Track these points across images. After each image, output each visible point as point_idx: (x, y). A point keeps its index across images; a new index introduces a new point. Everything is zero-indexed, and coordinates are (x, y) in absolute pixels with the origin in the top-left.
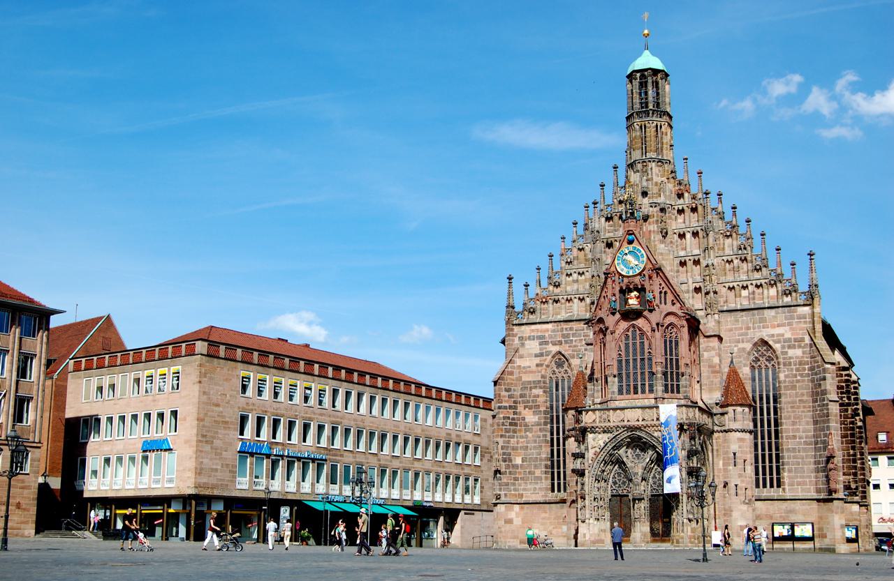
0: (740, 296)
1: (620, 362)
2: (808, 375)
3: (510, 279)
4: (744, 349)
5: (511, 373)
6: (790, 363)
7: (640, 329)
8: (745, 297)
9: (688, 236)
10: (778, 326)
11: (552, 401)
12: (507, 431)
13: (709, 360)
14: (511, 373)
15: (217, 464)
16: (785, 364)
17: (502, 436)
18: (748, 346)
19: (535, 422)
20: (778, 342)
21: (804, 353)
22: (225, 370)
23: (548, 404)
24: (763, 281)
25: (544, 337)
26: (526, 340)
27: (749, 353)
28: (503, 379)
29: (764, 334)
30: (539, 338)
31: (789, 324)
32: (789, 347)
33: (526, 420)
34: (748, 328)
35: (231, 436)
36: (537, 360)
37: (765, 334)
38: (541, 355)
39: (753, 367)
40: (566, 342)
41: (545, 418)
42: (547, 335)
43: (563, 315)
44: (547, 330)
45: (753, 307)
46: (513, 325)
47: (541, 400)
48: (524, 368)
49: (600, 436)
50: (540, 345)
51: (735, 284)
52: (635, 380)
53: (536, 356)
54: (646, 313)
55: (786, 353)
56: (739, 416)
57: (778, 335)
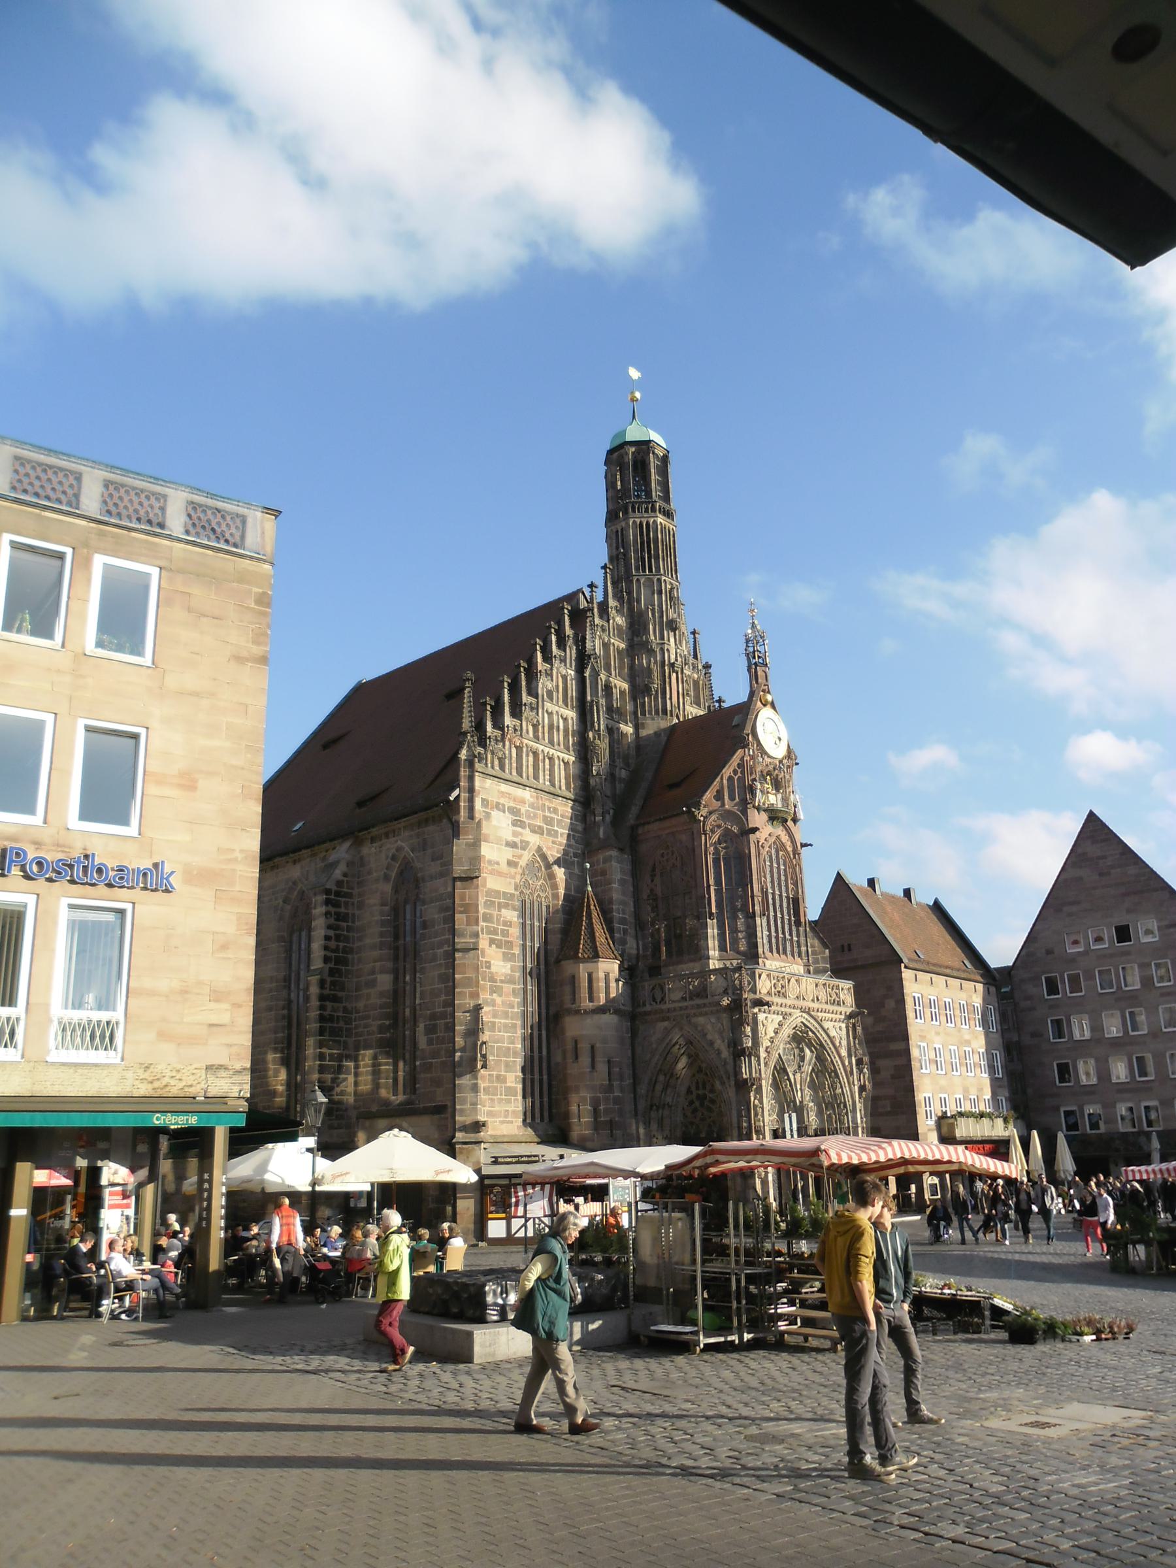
19: (506, 975)
26: (492, 808)
33: (494, 969)
36: (508, 853)
38: (513, 845)
40: (549, 833)
42: (523, 810)
44: (523, 802)
50: (514, 823)
53: (508, 844)
54: (790, 823)
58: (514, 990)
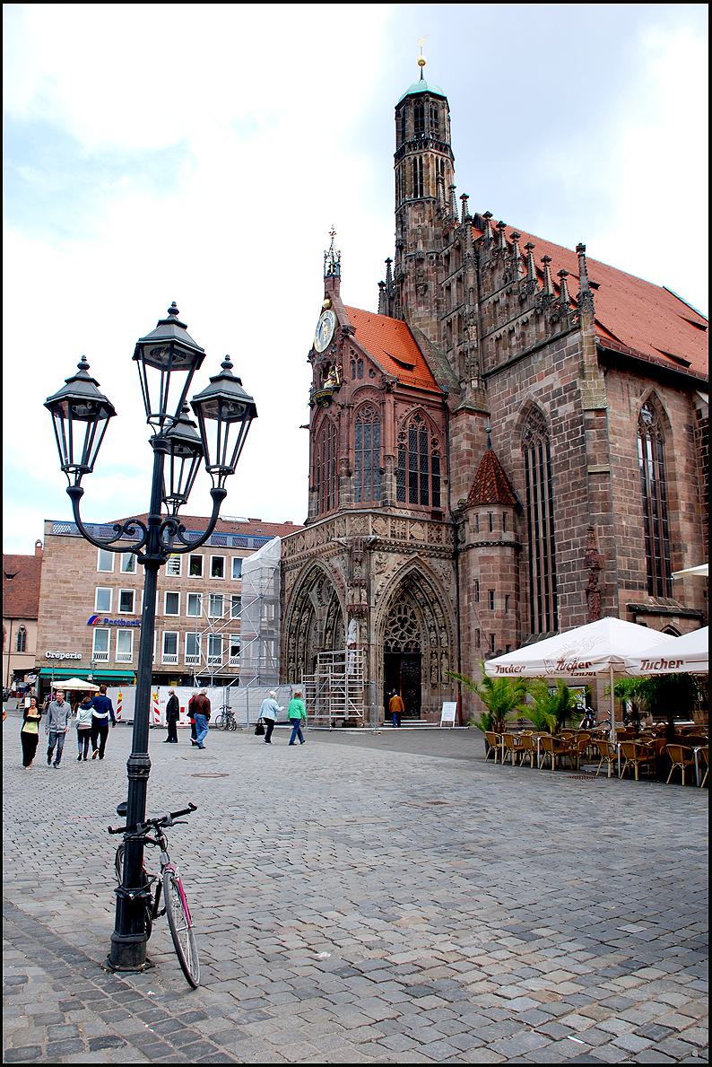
15: (65, 638)
18: (515, 416)
20: (544, 400)
22: (77, 548)
27: (518, 427)
34: (515, 390)
35: (85, 611)
39: (525, 448)
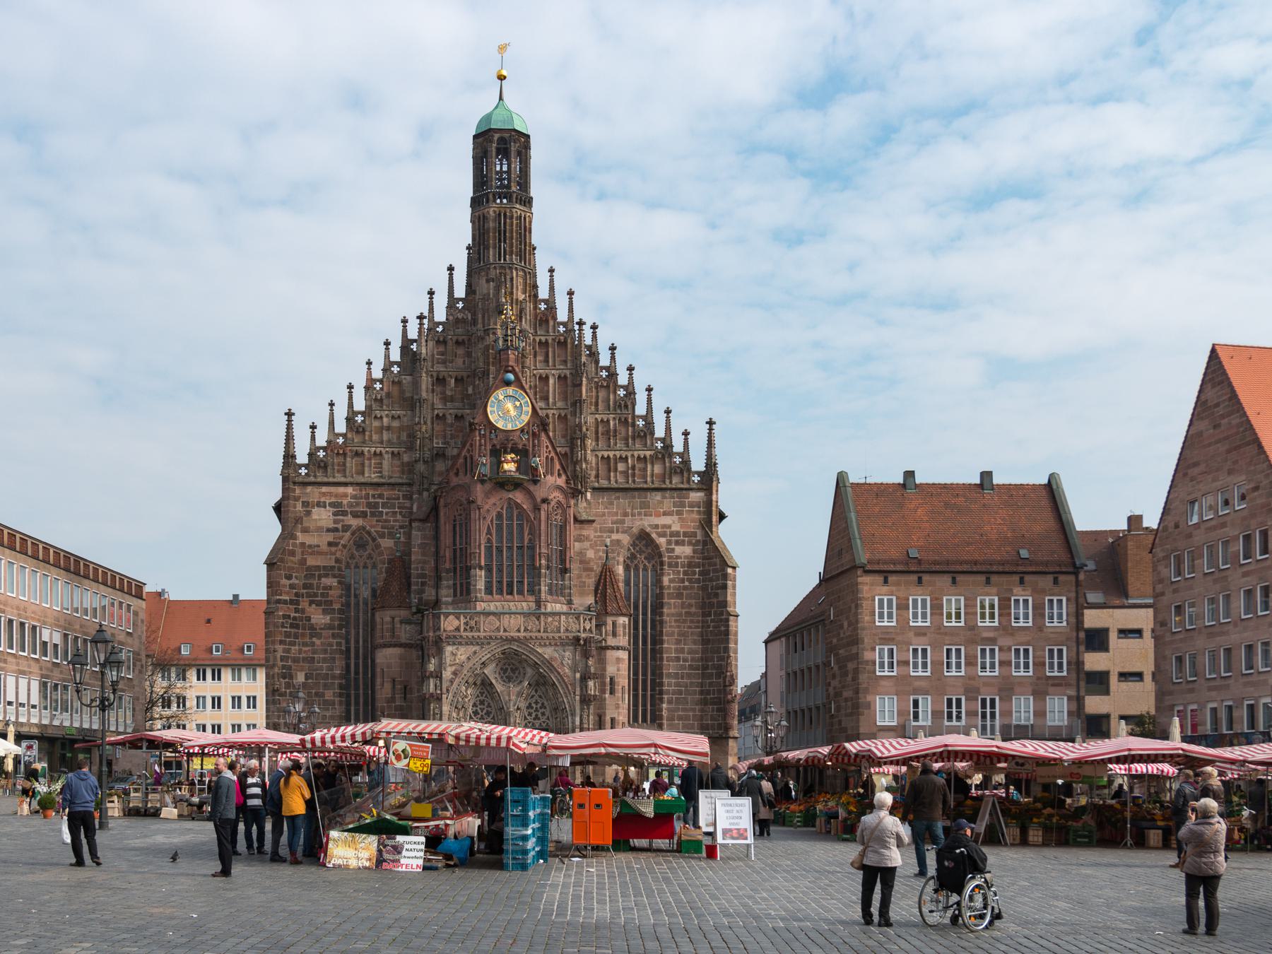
0: (616, 470)
1: (489, 549)
2: (698, 581)
3: (289, 414)
4: (618, 541)
5: (293, 553)
6: (676, 565)
7: (518, 506)
8: (621, 472)
9: (551, 381)
10: (665, 514)
11: (349, 596)
12: (287, 635)
13: (581, 553)
14: (293, 553)
16: (670, 565)
17: (281, 642)
18: (626, 539)
20: (660, 535)
21: (694, 551)
23: (343, 600)
24: (648, 453)
25: (340, 505)
28: (282, 560)
29: (646, 524)
30: (332, 505)
31: (679, 513)
32: (677, 543)
33: (313, 621)
34: (626, 514)
37: (647, 523)
38: (336, 530)
40: (373, 514)
41: (341, 619)
42: (345, 502)
43: (370, 475)
44: (345, 495)
45: (633, 486)
46: (295, 483)
47: (334, 593)
48: (310, 546)
49: (462, 649)
51: (611, 454)
52: (511, 575)
55: (673, 550)
56: (620, 630)
57: (664, 526)
58: (333, 634)
